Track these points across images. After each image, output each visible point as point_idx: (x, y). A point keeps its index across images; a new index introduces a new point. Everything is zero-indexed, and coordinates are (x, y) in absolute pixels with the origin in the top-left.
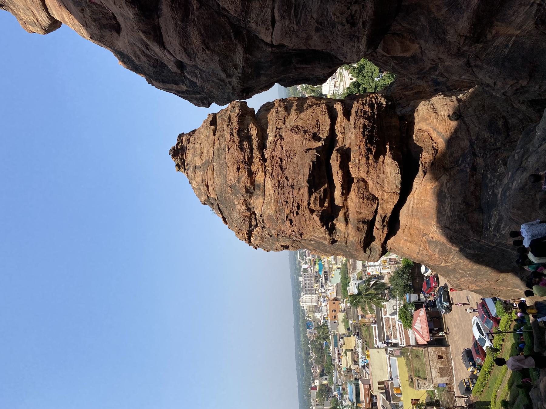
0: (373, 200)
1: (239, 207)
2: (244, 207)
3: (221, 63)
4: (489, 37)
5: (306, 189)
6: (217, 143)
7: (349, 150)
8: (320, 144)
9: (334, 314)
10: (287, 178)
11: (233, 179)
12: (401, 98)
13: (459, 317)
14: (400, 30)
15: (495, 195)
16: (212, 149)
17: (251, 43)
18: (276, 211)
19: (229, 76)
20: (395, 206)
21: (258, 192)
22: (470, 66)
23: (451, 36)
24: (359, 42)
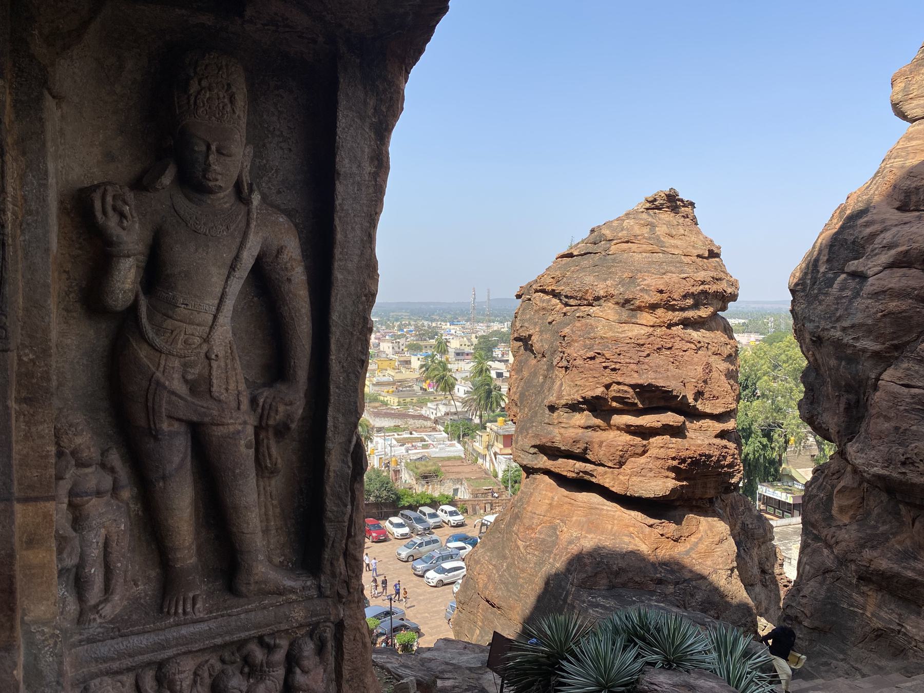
0: (620, 462)
2: (602, 293)
5: (640, 382)
6: (686, 260)
7: (684, 437)
8: (691, 400)
10: (648, 355)
11: (646, 282)
14: (867, 505)
17: (884, 359)
18: (602, 338)
19: (844, 329)
21: (625, 314)
22: (824, 573)
23: (867, 553)
24: (883, 468)
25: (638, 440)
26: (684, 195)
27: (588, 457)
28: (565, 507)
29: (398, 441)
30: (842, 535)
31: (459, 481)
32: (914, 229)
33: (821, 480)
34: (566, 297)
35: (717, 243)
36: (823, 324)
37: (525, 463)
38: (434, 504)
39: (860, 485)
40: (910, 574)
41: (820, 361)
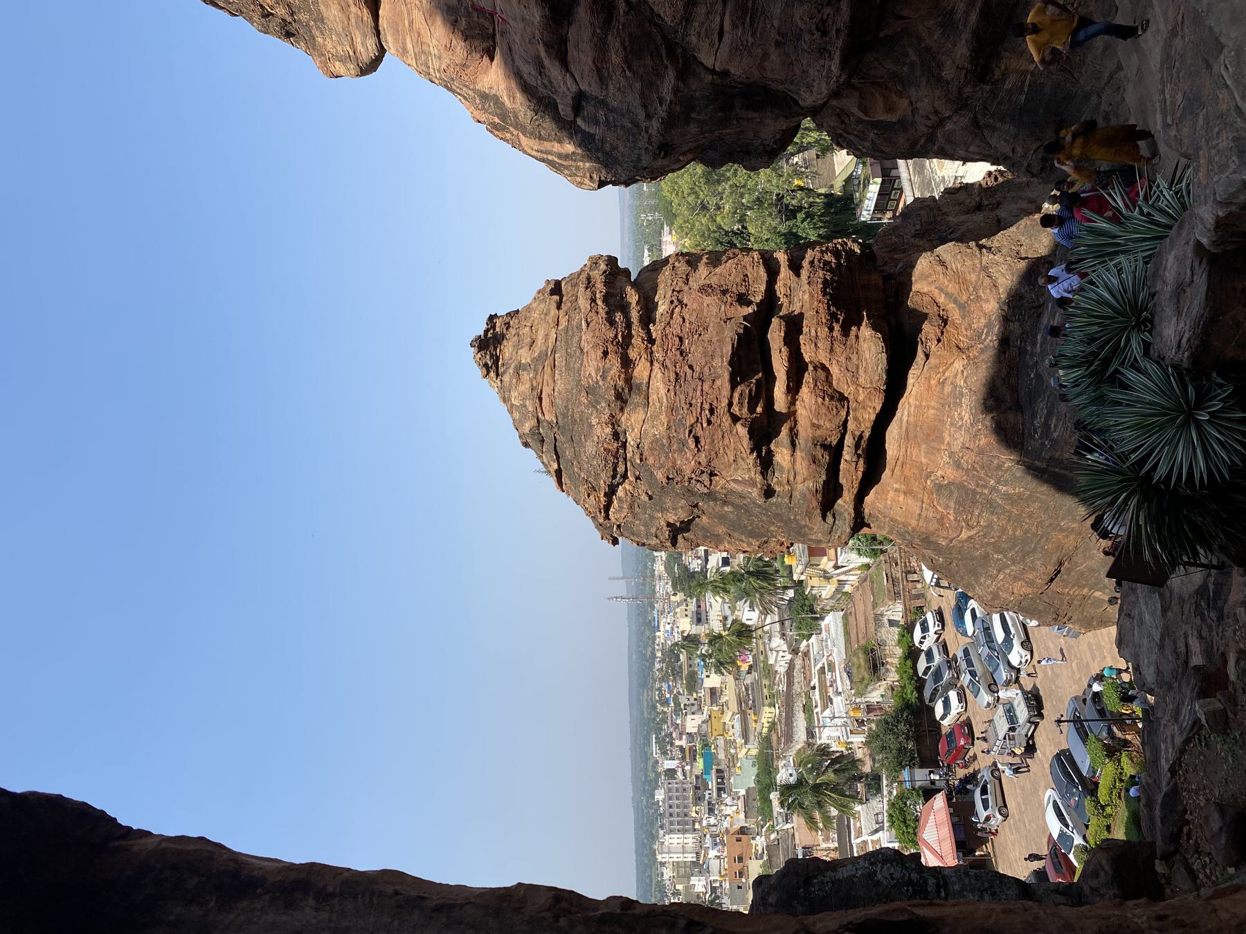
1: (599, 430)
2: (608, 430)
3: (642, 94)
4: (997, 74)
5: (727, 376)
6: (563, 323)
7: (801, 315)
8: (750, 310)
9: (738, 866)
10: (691, 367)
11: (593, 375)
12: (885, 264)
13: (1019, 804)
14: (882, 77)
15: (1038, 376)
16: (554, 330)
17: (687, 66)
19: (649, 117)
20: (878, 416)
21: (636, 399)
22: (979, 127)
23: (948, 73)
24: (831, 59)
25: (808, 377)
26: (480, 329)
27: (834, 443)
28: (907, 472)
29: (825, 707)
30: (925, 106)
31: (878, 618)
32: (517, 38)
33: (852, 137)
34: (614, 477)
35: (542, 285)
36: (642, 143)
37: (848, 530)
38: (912, 654)
39: (855, 88)
40: (973, 18)
41: (692, 145)
